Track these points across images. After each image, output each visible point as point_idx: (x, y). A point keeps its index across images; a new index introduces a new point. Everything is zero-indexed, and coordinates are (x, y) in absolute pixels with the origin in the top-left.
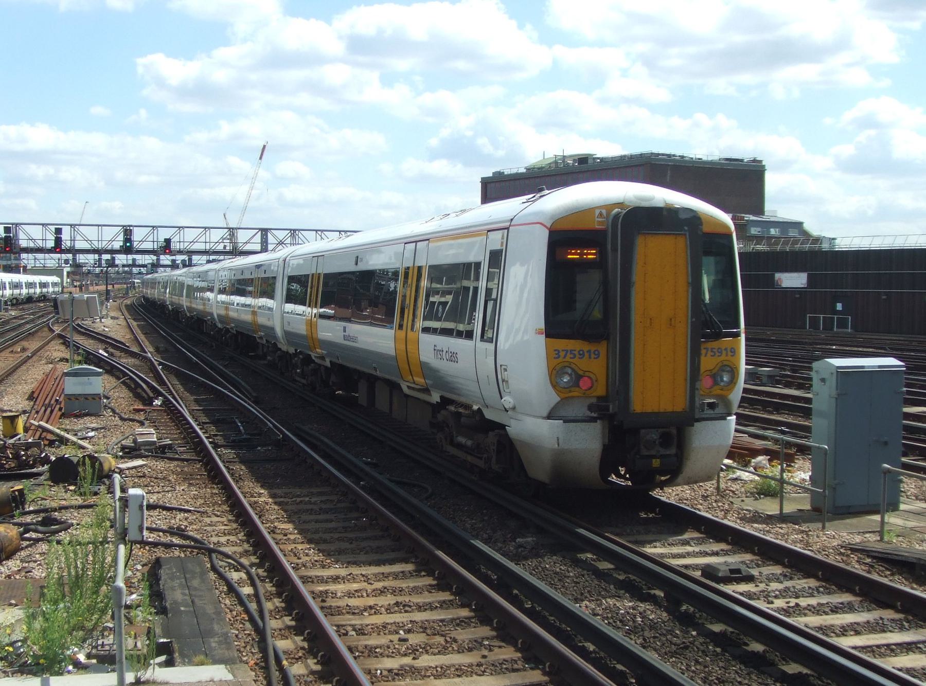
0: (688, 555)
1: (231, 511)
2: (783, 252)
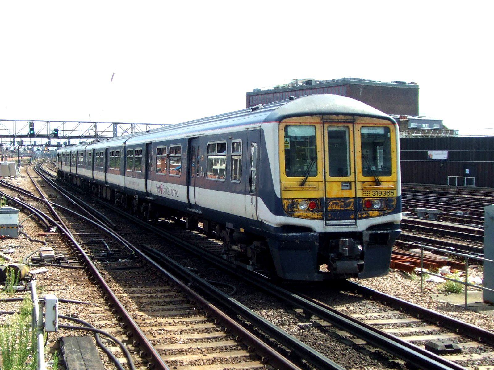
0: (412, 334)
1: (106, 303)
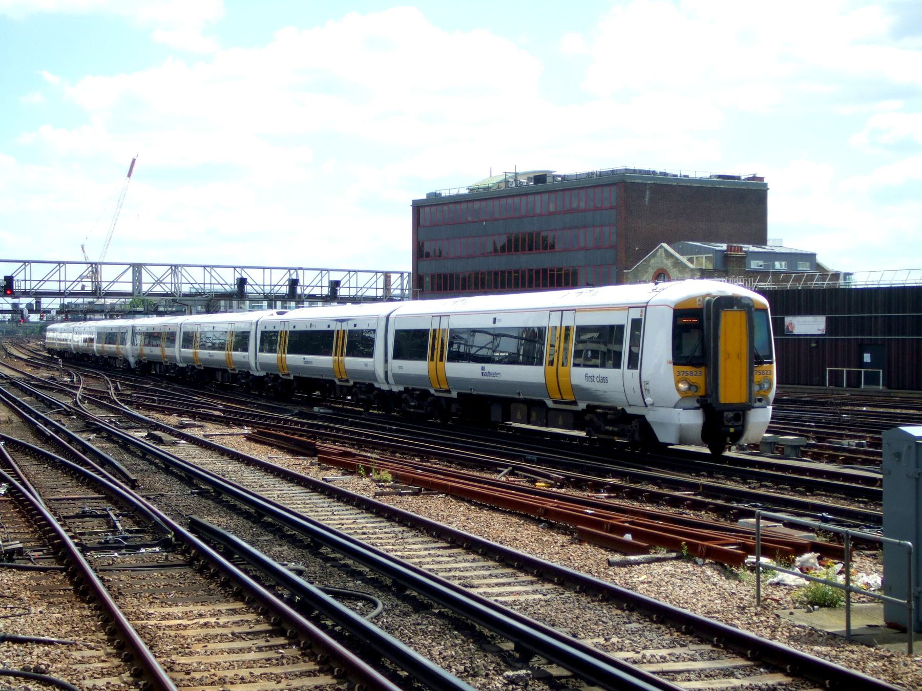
1: (110, 641)
2: (795, 290)
